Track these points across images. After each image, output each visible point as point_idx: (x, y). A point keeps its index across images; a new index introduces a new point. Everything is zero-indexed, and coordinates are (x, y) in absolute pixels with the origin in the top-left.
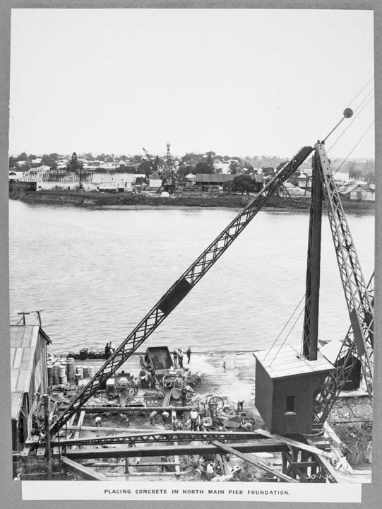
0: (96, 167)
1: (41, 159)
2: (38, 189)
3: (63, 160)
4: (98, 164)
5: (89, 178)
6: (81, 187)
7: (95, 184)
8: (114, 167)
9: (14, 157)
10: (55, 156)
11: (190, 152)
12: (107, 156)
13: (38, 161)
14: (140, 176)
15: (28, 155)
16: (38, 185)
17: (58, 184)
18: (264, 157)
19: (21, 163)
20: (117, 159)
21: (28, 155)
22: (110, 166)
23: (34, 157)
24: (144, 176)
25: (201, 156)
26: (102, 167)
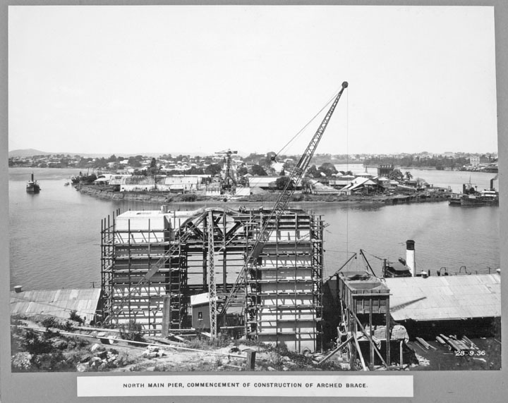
0: (171, 170)
2: (121, 190)
4: (173, 167)
5: (162, 181)
6: (156, 188)
7: (168, 185)
8: (188, 169)
9: (105, 158)
10: (140, 158)
11: (253, 152)
12: (184, 157)
13: (125, 162)
14: (206, 176)
15: (117, 157)
16: (122, 187)
17: (138, 186)
19: (111, 164)
20: (192, 159)
21: (117, 157)
22: (183, 168)
23: (122, 159)
24: (210, 176)
26: (177, 169)
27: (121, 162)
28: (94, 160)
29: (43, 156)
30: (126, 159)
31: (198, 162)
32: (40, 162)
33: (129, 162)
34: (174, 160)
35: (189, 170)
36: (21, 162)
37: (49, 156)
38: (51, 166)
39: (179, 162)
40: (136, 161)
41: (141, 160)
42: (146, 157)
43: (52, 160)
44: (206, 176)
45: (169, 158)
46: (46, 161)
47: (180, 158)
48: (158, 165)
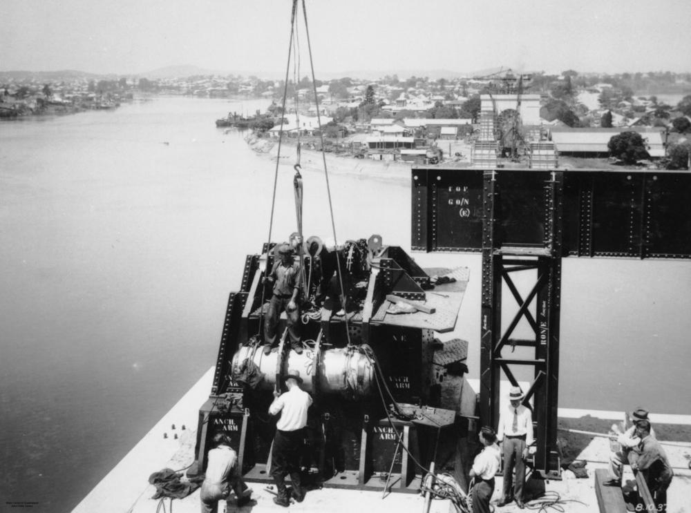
1: (328, 87)
3: (359, 87)
4: (403, 103)
10: (347, 82)
12: (419, 79)
18: (651, 74)
20: (432, 84)
25: (553, 78)
26: (409, 107)
27: (318, 89)
28: (277, 85)
29: (202, 78)
30: (326, 83)
31: (443, 89)
32: (197, 87)
33: (330, 90)
34: (402, 84)
35: (430, 110)
36: (170, 88)
37: (211, 77)
38: (213, 95)
39: (411, 89)
40: (340, 88)
41: (349, 85)
42: (358, 80)
43: (216, 85)
44: (462, 122)
45: (395, 82)
46: (206, 85)
47: (412, 83)
48: (377, 96)
